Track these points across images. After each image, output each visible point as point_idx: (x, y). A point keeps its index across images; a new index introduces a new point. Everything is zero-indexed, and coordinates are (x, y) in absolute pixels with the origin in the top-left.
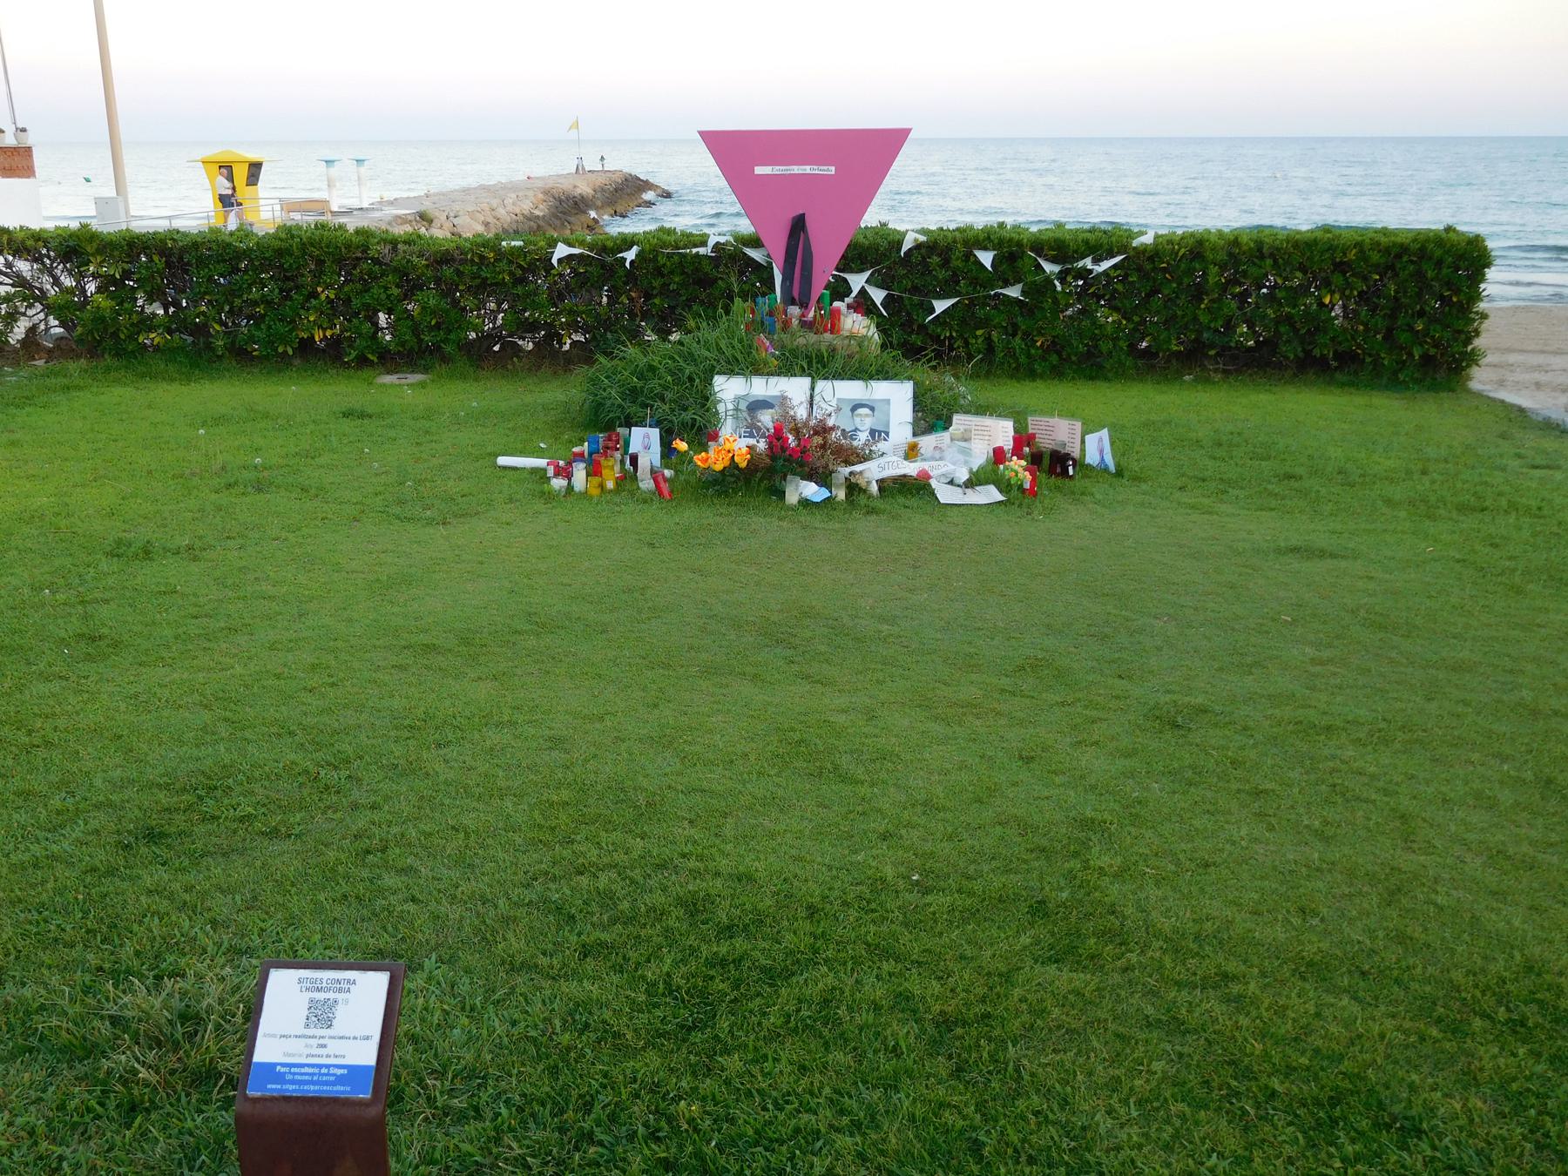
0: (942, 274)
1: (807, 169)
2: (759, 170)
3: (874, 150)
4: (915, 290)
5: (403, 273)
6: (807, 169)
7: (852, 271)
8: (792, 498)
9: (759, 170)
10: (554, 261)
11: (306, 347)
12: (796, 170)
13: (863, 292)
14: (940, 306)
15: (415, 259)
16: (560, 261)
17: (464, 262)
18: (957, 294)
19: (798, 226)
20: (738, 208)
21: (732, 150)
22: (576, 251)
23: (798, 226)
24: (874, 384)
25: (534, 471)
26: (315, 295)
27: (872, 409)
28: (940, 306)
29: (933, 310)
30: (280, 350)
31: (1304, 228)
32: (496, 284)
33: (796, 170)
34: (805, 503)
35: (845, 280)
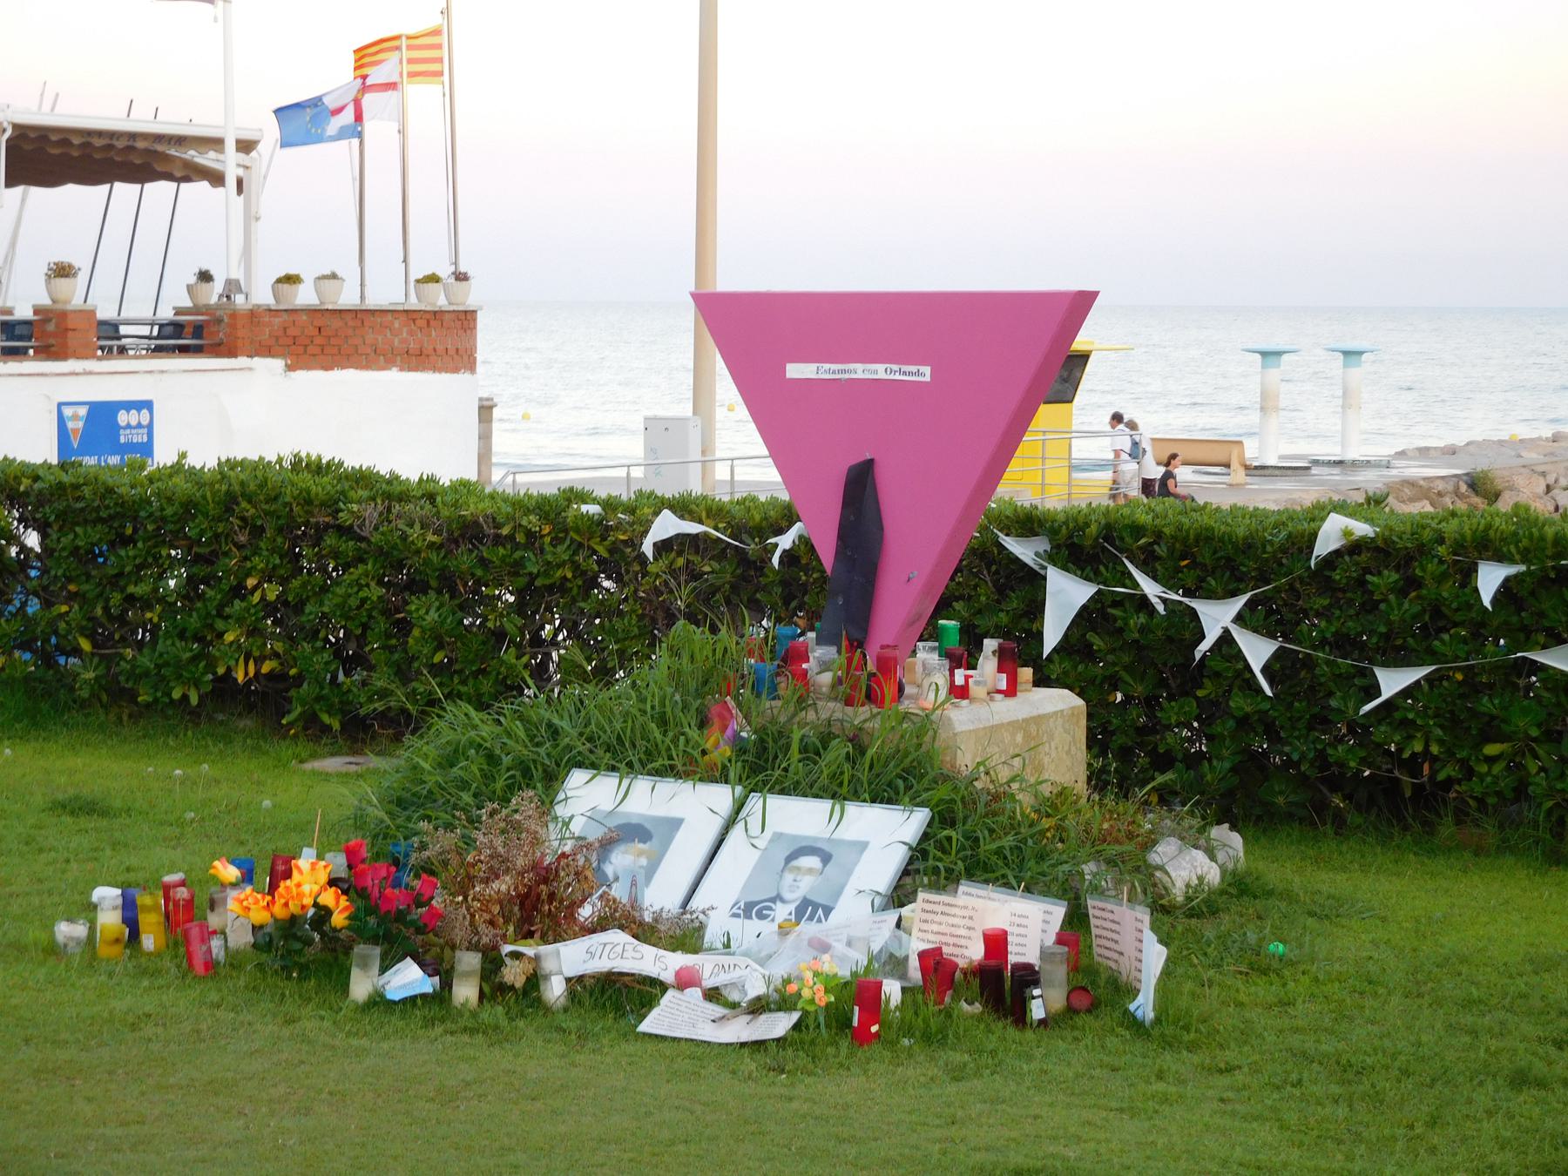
0: (1403, 610)
1: (880, 371)
2: (795, 371)
3: (1041, 345)
4: (1342, 643)
5: (392, 558)
6: (880, 371)
7: (1211, 595)
8: (361, 986)
9: (795, 371)
10: (647, 548)
11: (224, 689)
12: (860, 371)
13: (1226, 638)
14: (1392, 681)
15: (414, 533)
16: (663, 547)
17: (498, 540)
18: (1429, 656)
19: (860, 486)
20: (766, 452)
21: (751, 333)
22: (693, 528)
23: (860, 486)
24: (852, 809)
25: (850, 1020)
26: (239, 591)
27: (826, 858)
28: (1392, 681)
29: (1374, 690)
30: (176, 694)
31: (1273, 507)
32: (550, 589)
33: (860, 371)
34: (378, 1001)
35: (1194, 614)
